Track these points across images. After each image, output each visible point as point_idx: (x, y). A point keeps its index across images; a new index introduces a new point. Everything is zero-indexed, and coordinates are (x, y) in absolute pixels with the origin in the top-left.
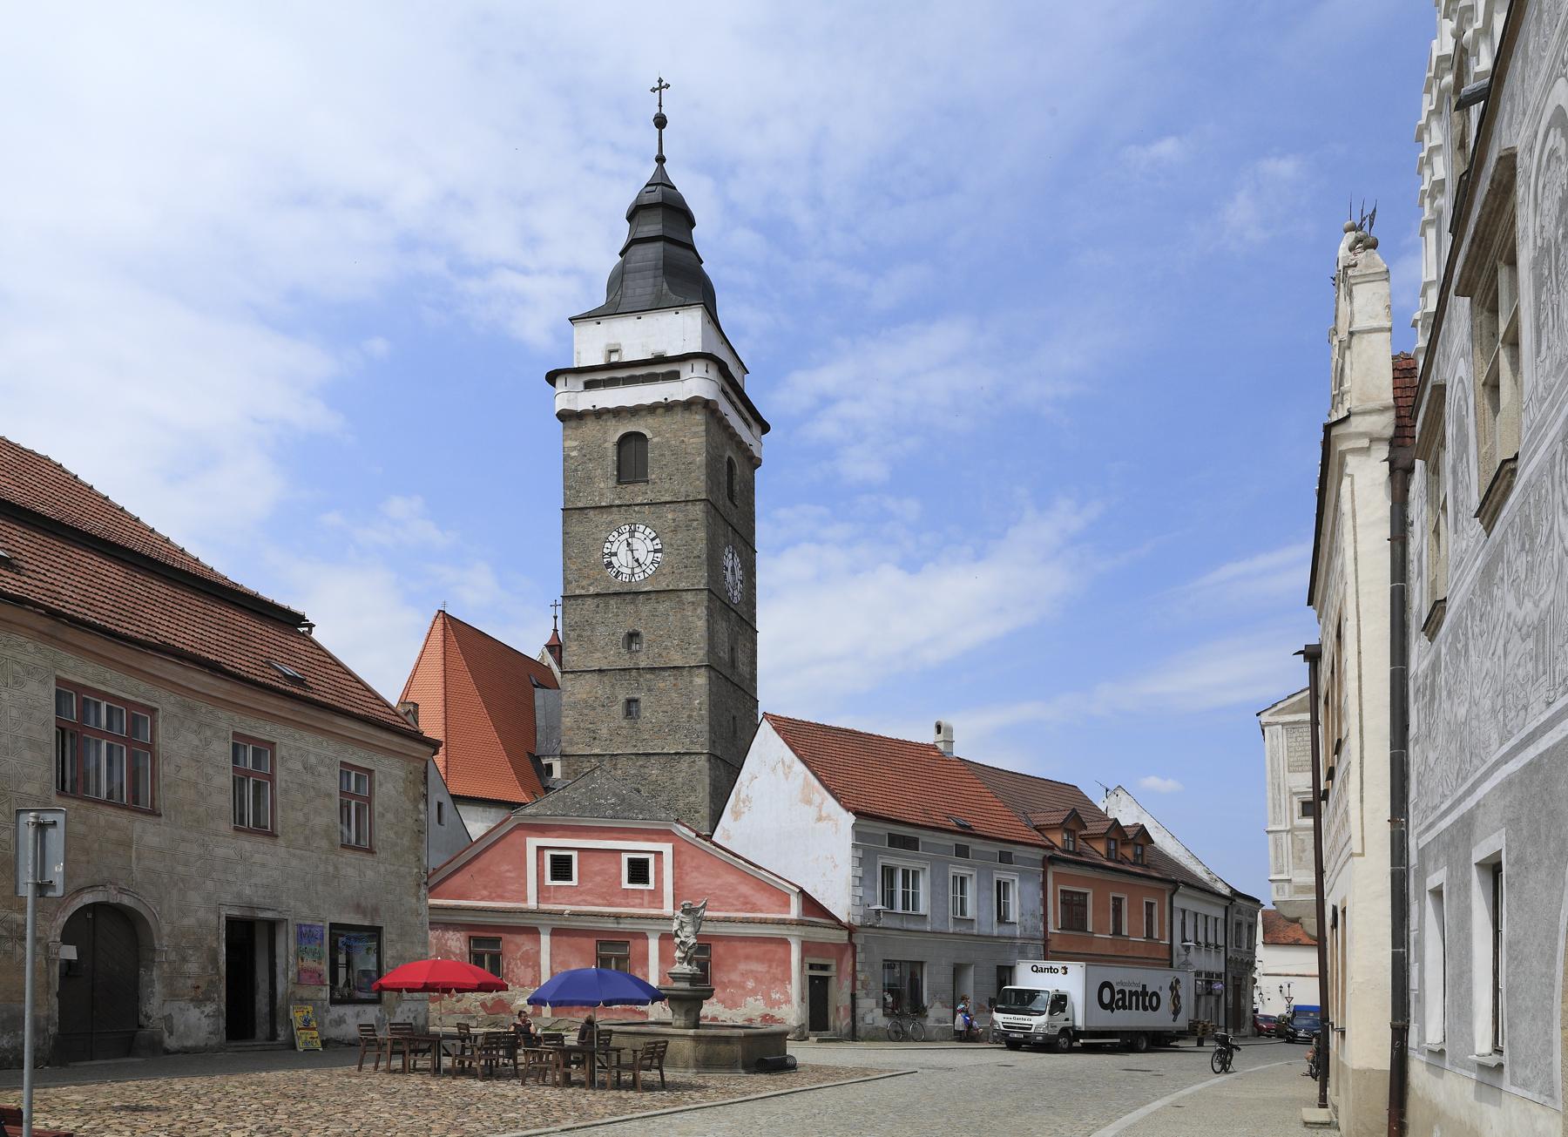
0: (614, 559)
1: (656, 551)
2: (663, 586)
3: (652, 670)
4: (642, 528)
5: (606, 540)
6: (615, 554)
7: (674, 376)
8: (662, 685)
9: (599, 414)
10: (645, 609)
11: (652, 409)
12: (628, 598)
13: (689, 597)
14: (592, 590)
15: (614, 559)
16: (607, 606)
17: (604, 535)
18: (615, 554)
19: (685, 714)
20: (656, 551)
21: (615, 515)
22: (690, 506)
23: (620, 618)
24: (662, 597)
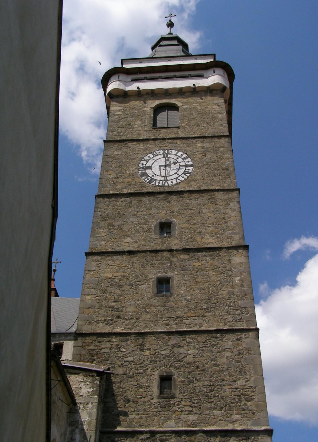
0: (148, 171)
1: (187, 166)
2: (196, 188)
3: (186, 251)
4: (174, 152)
5: (142, 159)
6: (150, 168)
7: (201, 76)
8: (197, 264)
9: (139, 94)
10: (177, 203)
11: (181, 92)
12: (161, 197)
13: (221, 195)
14: (125, 191)
15: (148, 171)
16: (140, 202)
17: (139, 156)
18: (150, 168)
19: (224, 293)
20: (187, 166)
21: (151, 145)
22: (216, 140)
23: (154, 211)
24: (193, 196)
